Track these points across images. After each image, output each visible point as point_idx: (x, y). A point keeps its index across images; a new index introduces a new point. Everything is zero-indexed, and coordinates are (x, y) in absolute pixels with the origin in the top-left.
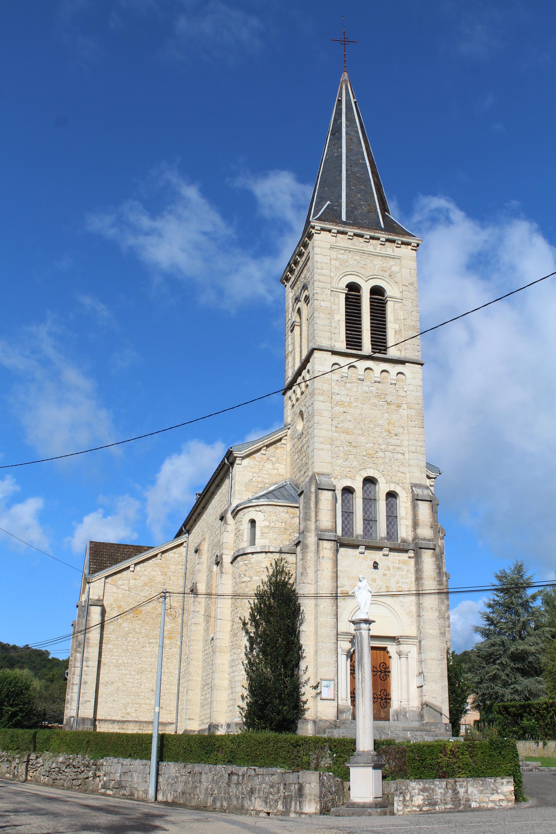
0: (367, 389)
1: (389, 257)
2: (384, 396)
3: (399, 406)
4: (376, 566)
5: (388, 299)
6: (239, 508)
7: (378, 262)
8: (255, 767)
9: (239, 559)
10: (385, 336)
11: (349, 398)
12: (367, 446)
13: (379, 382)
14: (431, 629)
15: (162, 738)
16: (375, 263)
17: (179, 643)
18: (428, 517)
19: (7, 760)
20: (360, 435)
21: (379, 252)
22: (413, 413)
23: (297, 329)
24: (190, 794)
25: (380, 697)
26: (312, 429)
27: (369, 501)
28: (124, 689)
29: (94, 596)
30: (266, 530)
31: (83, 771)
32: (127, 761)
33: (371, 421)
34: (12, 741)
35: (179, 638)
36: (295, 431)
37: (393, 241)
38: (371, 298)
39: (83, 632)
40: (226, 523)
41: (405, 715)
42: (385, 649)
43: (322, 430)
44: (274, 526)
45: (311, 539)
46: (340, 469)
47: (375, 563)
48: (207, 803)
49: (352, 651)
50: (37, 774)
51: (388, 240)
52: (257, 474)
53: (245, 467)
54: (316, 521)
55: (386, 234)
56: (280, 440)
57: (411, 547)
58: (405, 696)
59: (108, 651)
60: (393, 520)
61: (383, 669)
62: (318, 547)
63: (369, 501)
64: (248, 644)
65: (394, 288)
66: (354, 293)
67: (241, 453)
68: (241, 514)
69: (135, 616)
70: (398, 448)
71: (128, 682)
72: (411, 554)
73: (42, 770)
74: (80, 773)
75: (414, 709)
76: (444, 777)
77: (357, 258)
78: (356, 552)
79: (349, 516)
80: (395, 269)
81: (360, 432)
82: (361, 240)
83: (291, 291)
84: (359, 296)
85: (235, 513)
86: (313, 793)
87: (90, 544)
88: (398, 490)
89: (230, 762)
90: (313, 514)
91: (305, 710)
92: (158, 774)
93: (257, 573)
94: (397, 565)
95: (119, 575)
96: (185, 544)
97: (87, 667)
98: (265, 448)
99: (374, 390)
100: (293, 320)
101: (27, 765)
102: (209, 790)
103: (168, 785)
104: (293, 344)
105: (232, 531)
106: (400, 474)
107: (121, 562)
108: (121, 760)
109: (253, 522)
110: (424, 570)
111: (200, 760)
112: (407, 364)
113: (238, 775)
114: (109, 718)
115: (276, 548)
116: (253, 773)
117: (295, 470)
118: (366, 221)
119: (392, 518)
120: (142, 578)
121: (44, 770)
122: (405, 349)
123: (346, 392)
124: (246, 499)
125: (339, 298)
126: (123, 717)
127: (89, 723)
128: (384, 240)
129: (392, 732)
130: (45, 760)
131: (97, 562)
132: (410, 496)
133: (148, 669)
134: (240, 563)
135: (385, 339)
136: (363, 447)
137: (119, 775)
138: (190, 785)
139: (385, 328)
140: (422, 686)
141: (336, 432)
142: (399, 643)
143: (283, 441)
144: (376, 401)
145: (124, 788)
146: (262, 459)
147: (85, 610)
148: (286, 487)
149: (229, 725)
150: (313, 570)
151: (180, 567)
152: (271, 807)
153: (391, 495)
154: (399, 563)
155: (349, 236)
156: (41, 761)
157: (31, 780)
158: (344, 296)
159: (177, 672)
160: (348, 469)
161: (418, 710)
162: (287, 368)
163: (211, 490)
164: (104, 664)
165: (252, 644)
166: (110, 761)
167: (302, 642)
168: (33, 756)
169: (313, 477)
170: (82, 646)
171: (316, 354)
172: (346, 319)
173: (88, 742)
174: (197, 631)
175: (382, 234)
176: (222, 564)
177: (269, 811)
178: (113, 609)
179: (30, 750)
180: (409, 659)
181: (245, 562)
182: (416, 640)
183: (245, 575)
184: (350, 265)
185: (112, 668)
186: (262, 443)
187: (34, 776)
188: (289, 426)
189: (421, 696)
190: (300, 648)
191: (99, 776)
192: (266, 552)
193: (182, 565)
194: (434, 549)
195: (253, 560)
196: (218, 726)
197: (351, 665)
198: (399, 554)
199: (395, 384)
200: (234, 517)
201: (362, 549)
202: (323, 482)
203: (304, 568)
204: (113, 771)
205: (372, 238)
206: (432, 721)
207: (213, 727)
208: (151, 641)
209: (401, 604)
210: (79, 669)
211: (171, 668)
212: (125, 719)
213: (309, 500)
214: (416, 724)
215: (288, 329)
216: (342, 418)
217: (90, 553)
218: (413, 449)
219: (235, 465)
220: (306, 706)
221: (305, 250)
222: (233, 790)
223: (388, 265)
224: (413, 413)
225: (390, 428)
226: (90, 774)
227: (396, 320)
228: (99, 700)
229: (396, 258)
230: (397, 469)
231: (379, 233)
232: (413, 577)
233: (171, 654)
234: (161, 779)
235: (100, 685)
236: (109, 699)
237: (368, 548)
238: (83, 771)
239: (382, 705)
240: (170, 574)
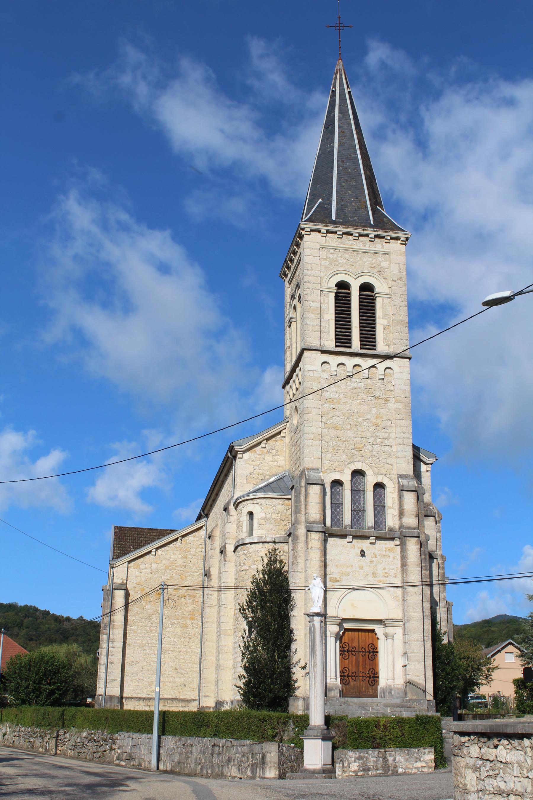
0: (355, 385)
1: (378, 253)
3: (387, 400)
4: (363, 554)
5: (376, 295)
6: (239, 501)
7: (367, 259)
8: (232, 740)
9: (239, 548)
10: (374, 331)
11: (338, 395)
12: (356, 440)
13: (368, 378)
14: (414, 612)
15: (164, 715)
16: (364, 260)
17: (200, 623)
18: (413, 506)
19: (40, 736)
20: (348, 430)
21: (368, 249)
22: (401, 407)
23: (293, 324)
24: (184, 763)
25: (368, 675)
26: (302, 426)
27: (357, 493)
28: (149, 668)
29: (118, 580)
30: (263, 522)
31: (102, 745)
32: (136, 735)
33: (359, 416)
34: (44, 719)
35: (200, 619)
36: (292, 424)
37: (382, 237)
38: (360, 295)
39: (108, 615)
40: (229, 514)
41: (390, 692)
42: (373, 631)
43: (312, 428)
44: (270, 517)
45: (301, 530)
46: (329, 463)
47: (362, 551)
48: (196, 771)
49: (341, 633)
50: (64, 748)
51: (376, 237)
52: (258, 466)
53: (246, 460)
54: (306, 514)
55: (374, 231)
56: (280, 433)
57: (397, 535)
58: (391, 675)
59: (133, 632)
60: (381, 509)
61: (371, 650)
62: (307, 538)
63: (357, 493)
64: (247, 628)
65: (383, 284)
66: (344, 291)
67: (242, 447)
68: (240, 506)
69: (157, 598)
70: (386, 441)
71: (152, 661)
72: (397, 542)
73: (69, 745)
74: (100, 747)
75: (399, 687)
76: (377, 748)
77: (347, 256)
78: (344, 541)
79: (338, 507)
80: (384, 264)
81: (348, 427)
82: (351, 238)
83: (289, 286)
84: (350, 294)
85: (237, 505)
86: (273, 760)
87: (115, 529)
88: (385, 481)
89: (215, 735)
90: (303, 507)
91: (295, 689)
92: (159, 747)
93: (255, 562)
94: (384, 553)
95: (141, 560)
96: (204, 528)
97: (113, 647)
98: (265, 442)
99: (363, 386)
100: (291, 316)
101: (57, 740)
102: (198, 759)
103: (167, 755)
104: (291, 339)
105: (234, 521)
106: (387, 466)
107: (144, 546)
108: (131, 734)
109: (251, 514)
110: (409, 557)
111: (193, 734)
113: (219, 746)
114: (135, 695)
115: (272, 538)
116: (229, 744)
117: (292, 462)
118: (356, 218)
119: (380, 507)
120: (164, 562)
121: (71, 744)
122: (394, 344)
124: (247, 491)
125: (328, 297)
126: (148, 695)
127: (116, 700)
128: (373, 236)
129: (372, 708)
130: (72, 735)
131: (121, 547)
132: (397, 486)
133: (171, 649)
134: (240, 552)
135: (375, 335)
136: (351, 442)
137: (130, 747)
138: (184, 756)
139: (375, 324)
140: (406, 666)
141: (325, 428)
142: (385, 626)
143: (282, 434)
144: (364, 396)
145: (134, 759)
146: (263, 452)
147: (110, 594)
148: (284, 479)
149: (232, 702)
150: (303, 559)
151: (200, 550)
152: (242, 774)
153: (379, 486)
154: (385, 551)
155: (338, 235)
156: (68, 736)
157: (60, 754)
158: (334, 295)
159: (199, 651)
160: (337, 463)
161: (403, 688)
162: (286, 362)
163: (221, 478)
164: (129, 645)
165: (251, 628)
166: (123, 736)
167: (292, 626)
168: (61, 732)
169: (303, 472)
170: (108, 628)
171: (306, 354)
172: (336, 317)
173: (107, 718)
174: (211, 613)
175: (371, 231)
176: (225, 553)
177: (241, 777)
178: (136, 592)
179: (59, 726)
180: (395, 640)
181: (245, 552)
182: (401, 623)
183: (244, 564)
184: (339, 263)
185: (136, 648)
186: (261, 437)
187: (63, 750)
188: (287, 420)
189: (405, 675)
190: (291, 631)
191: (114, 749)
192: (263, 543)
193: (202, 548)
194: (419, 537)
195: (251, 550)
196: (223, 703)
197: (340, 647)
198: (386, 542)
199: (384, 379)
200: (236, 509)
201: (349, 538)
202: (311, 477)
203: (295, 558)
204: (125, 745)
205: (361, 235)
206: (415, 697)
207: (219, 704)
208: (173, 621)
210: (105, 649)
211: (193, 647)
212: (150, 696)
213: (300, 494)
214: (398, 701)
215: (287, 324)
216: (331, 414)
217: (114, 539)
218: (400, 441)
219: (237, 459)
220: (296, 685)
221: (298, 249)
222: (215, 759)
223: (378, 261)
224: (401, 407)
225: (378, 421)
226: (108, 747)
227: (385, 315)
228: (125, 679)
229: (386, 254)
230: (384, 461)
231: (368, 230)
232: (398, 563)
233: (192, 634)
234: (162, 751)
235: (126, 665)
236: (134, 678)
237: (355, 537)
238: (102, 745)
240: (190, 557)
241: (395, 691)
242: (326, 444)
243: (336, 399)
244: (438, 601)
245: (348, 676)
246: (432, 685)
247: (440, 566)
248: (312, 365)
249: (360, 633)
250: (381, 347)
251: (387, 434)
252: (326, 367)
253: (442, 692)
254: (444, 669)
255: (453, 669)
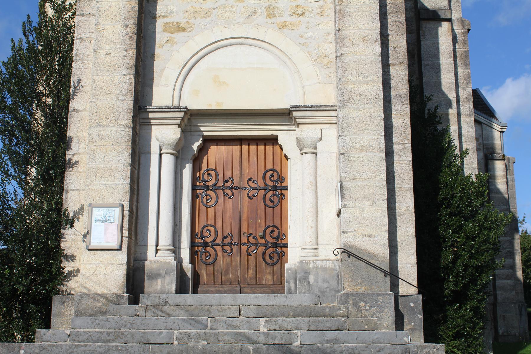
14: (361, 83)
25: (262, 241)
41: (305, 279)
42: (273, 140)
61: (270, 183)
75: (328, 264)
206: (362, 290)
209: (302, 41)
239: (268, 259)
241: (317, 274)
244: (452, 96)
245: (214, 244)
246: (413, 259)
247: (460, 38)
249: (245, 147)
253: (457, 276)
254: (460, 227)
255: (481, 226)
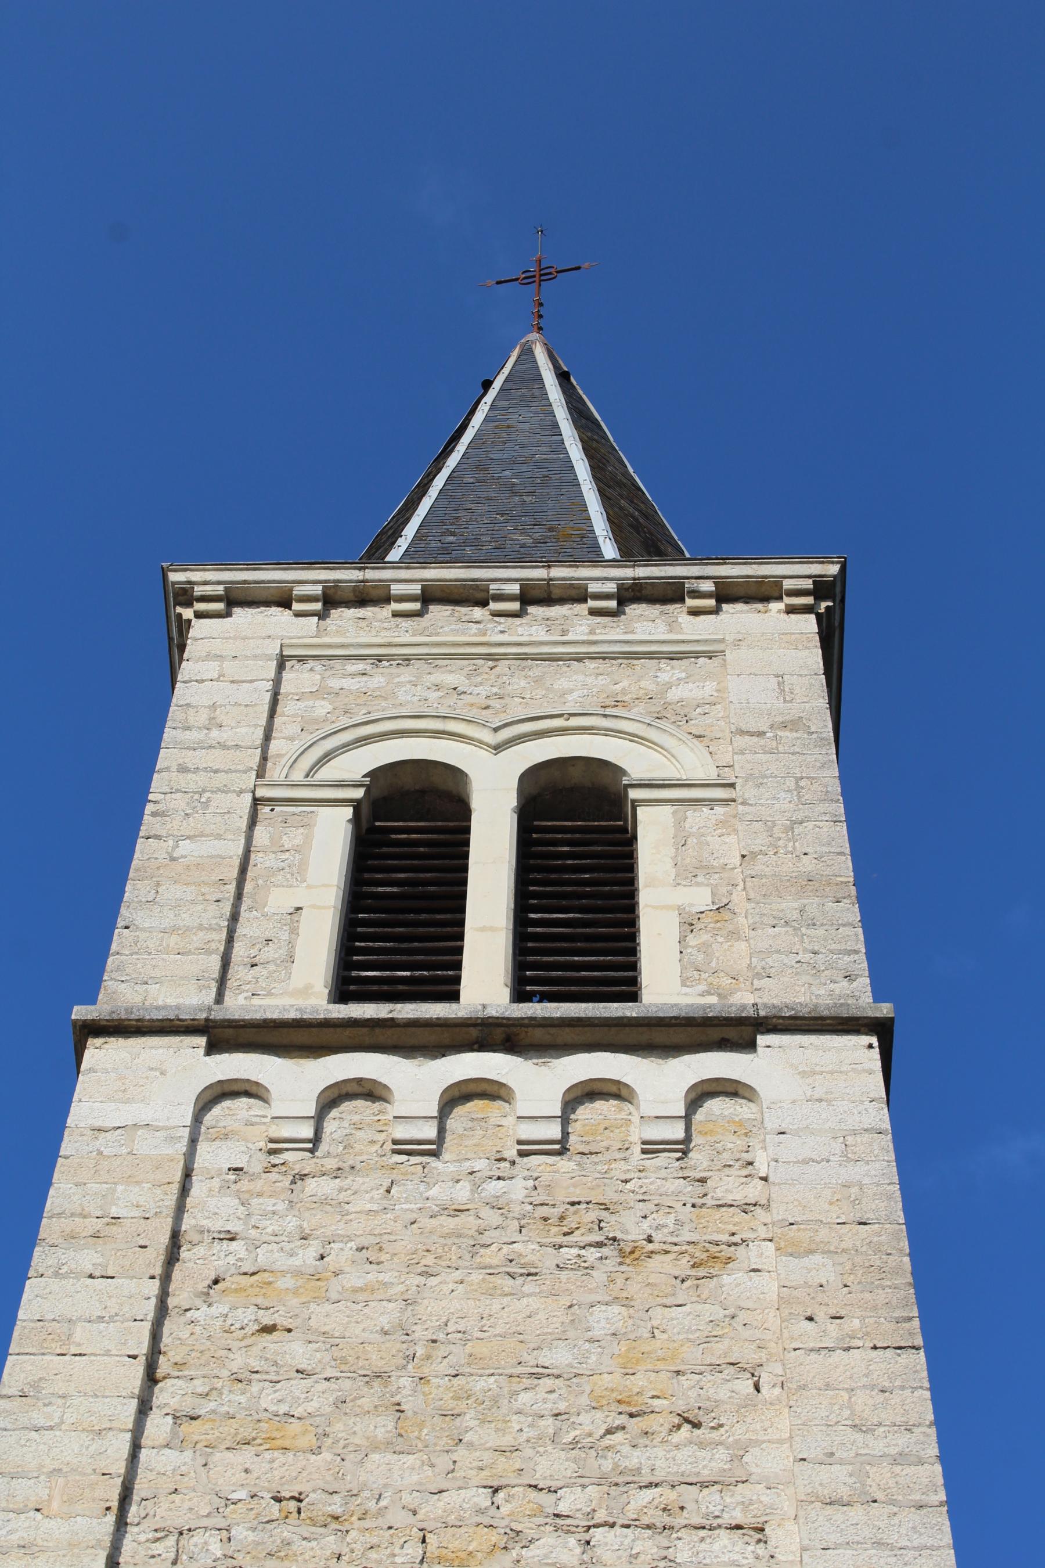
0: (462, 1193)
1: (651, 656)
2: (594, 1214)
3: (711, 1259)
11: (313, 1249)
12: (433, 1509)
70: (710, 1500)
77: (451, 679)
112: (762, 1040)
123: (291, 1223)
199: (684, 1147)
216: (238, 1361)
229: (697, 654)
242: (166, 1548)
243: (297, 1273)
248: (128, 1101)
250: (664, 982)
251: (722, 1453)
252: (243, 1114)
